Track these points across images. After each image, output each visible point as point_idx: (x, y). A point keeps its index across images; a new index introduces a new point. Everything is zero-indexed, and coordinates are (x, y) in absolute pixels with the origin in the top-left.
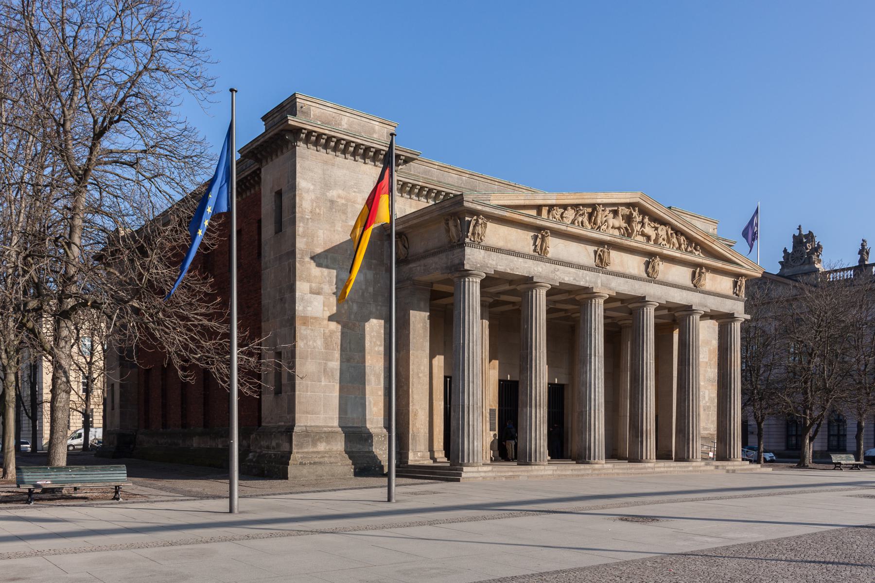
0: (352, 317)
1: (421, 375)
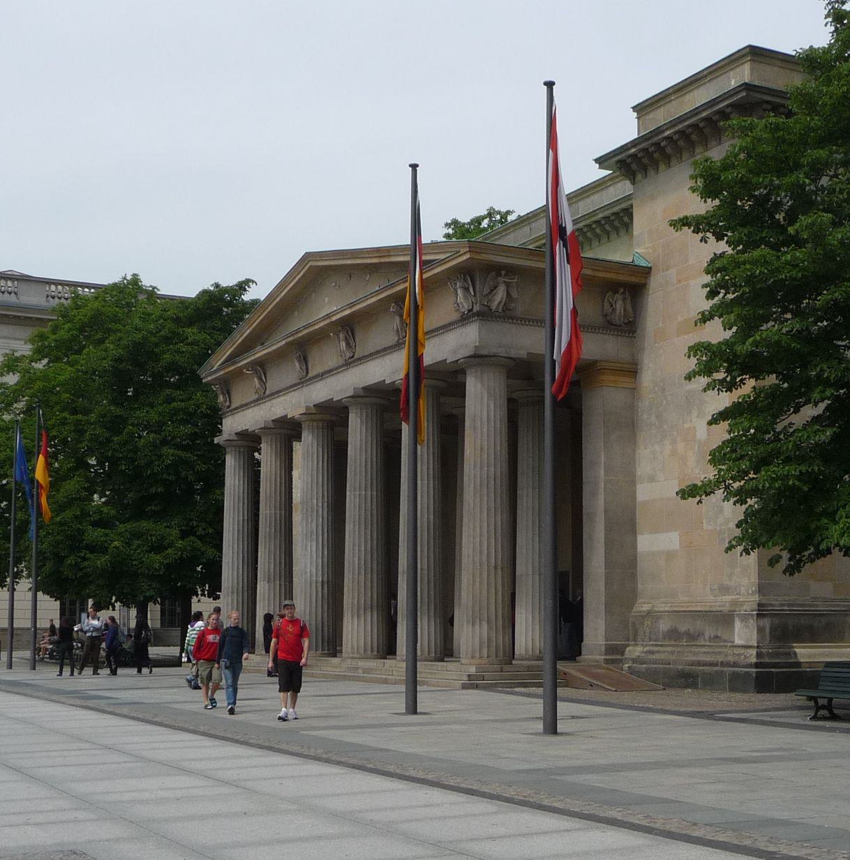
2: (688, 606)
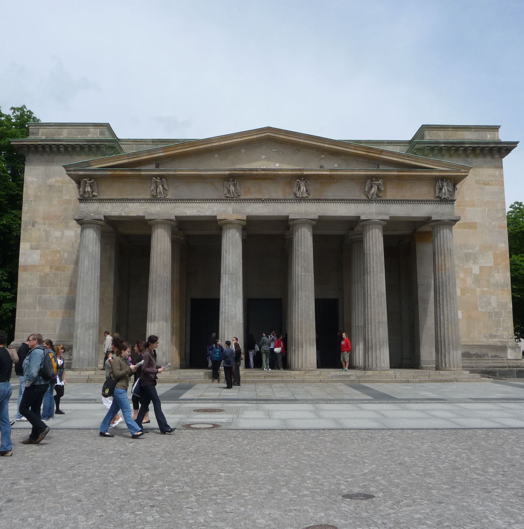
0: (63, 262)
2: (472, 343)
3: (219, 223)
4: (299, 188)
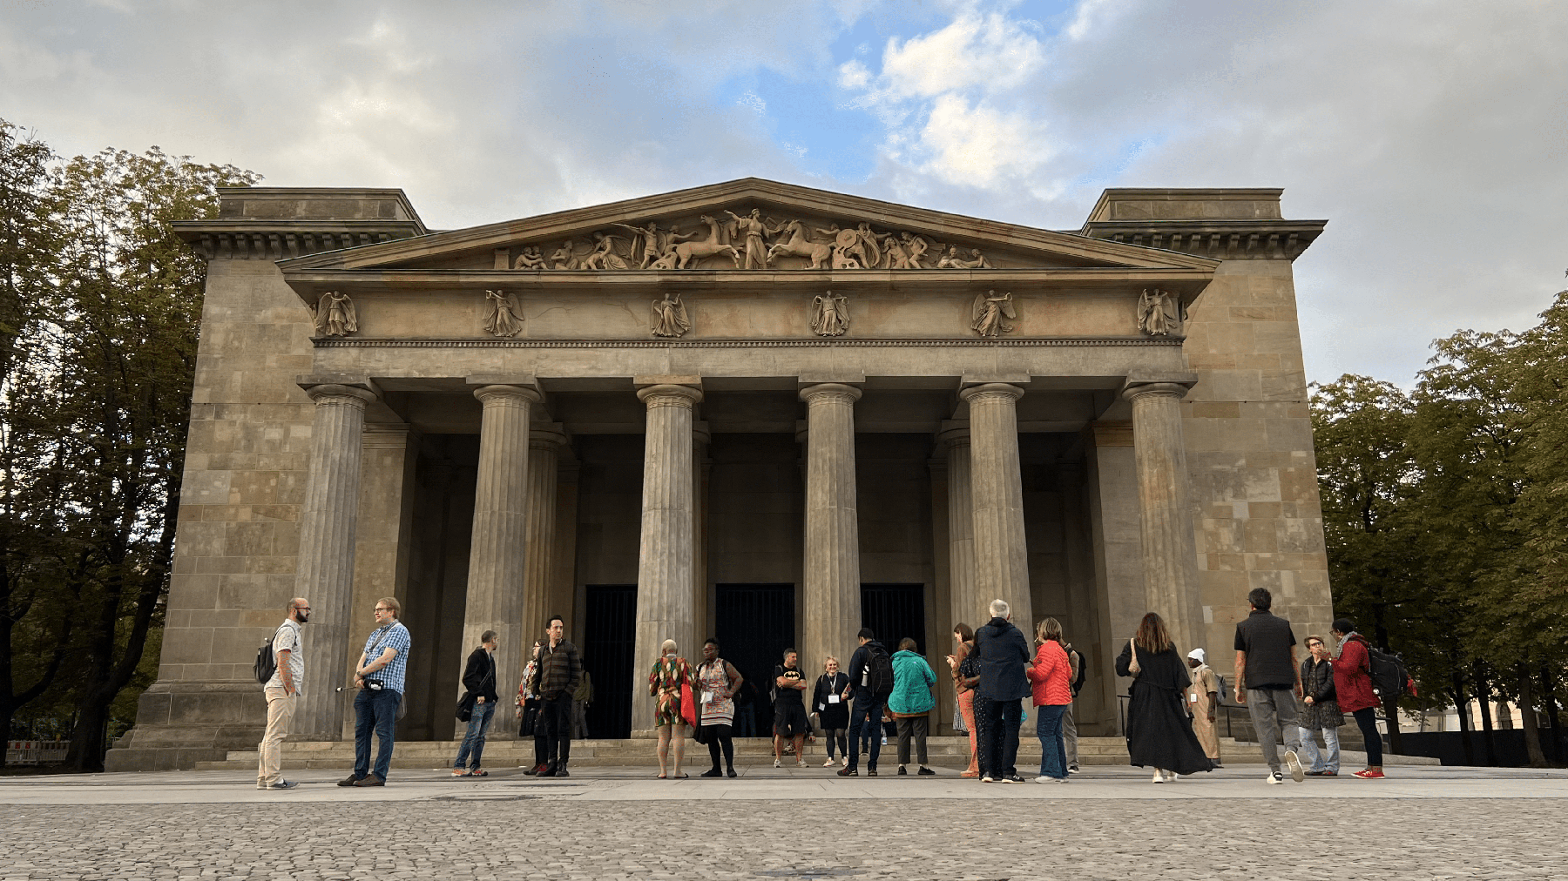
1: (376, 582)
3: (639, 393)
4: (822, 314)
